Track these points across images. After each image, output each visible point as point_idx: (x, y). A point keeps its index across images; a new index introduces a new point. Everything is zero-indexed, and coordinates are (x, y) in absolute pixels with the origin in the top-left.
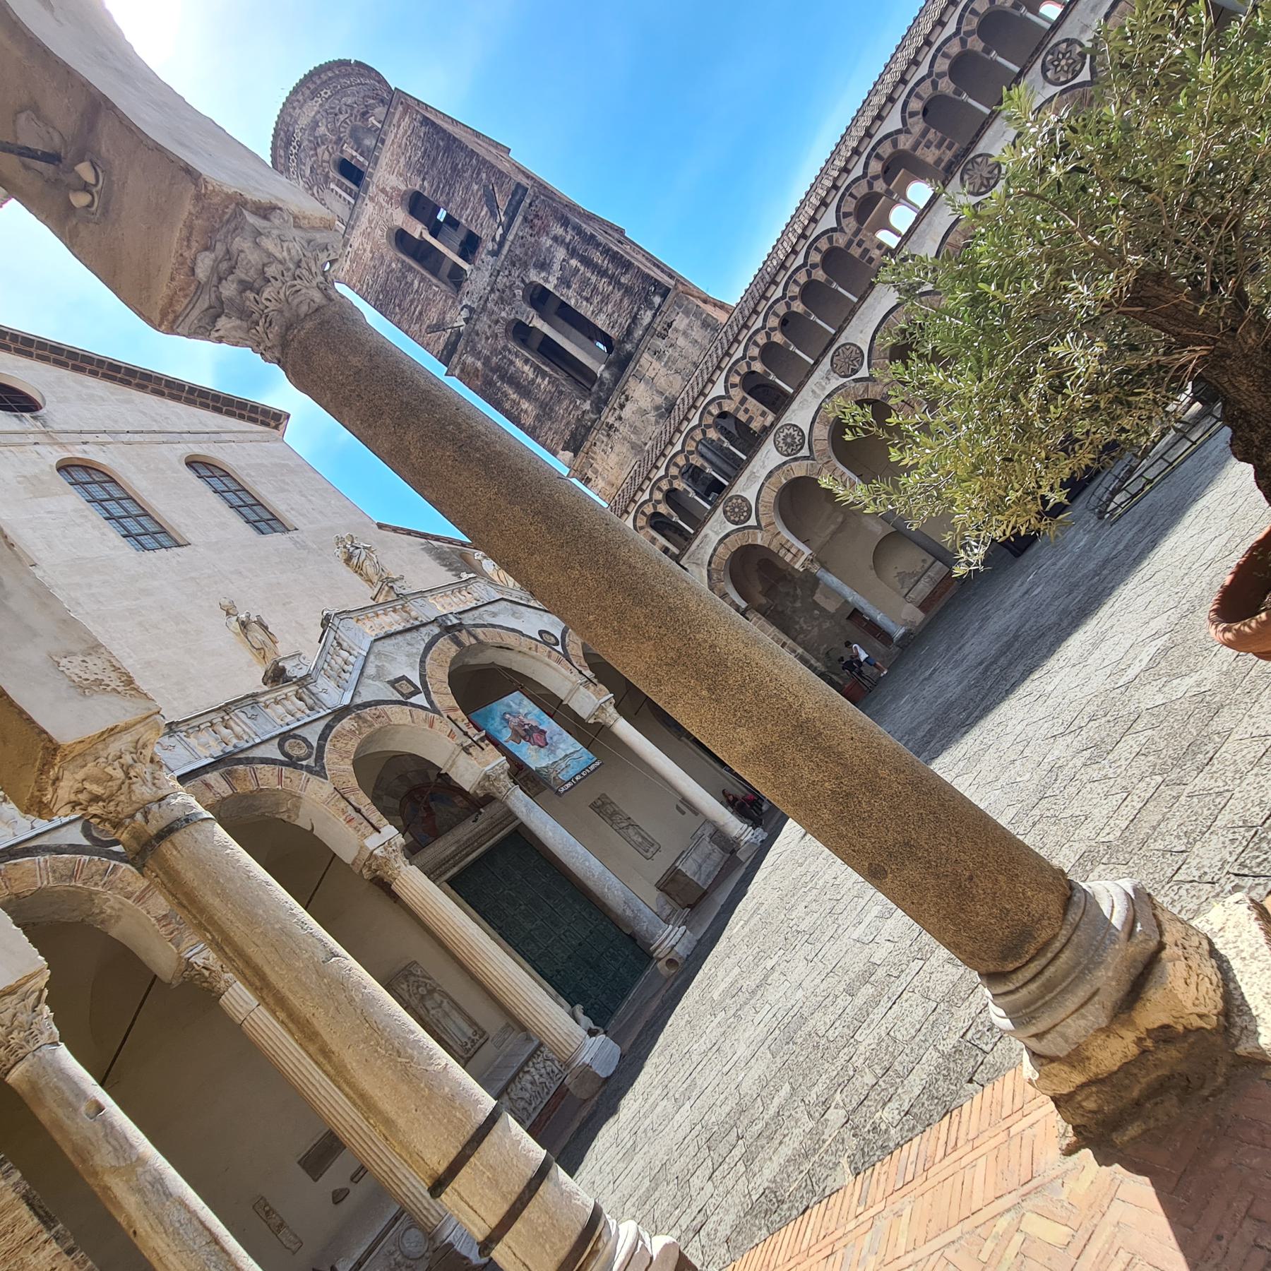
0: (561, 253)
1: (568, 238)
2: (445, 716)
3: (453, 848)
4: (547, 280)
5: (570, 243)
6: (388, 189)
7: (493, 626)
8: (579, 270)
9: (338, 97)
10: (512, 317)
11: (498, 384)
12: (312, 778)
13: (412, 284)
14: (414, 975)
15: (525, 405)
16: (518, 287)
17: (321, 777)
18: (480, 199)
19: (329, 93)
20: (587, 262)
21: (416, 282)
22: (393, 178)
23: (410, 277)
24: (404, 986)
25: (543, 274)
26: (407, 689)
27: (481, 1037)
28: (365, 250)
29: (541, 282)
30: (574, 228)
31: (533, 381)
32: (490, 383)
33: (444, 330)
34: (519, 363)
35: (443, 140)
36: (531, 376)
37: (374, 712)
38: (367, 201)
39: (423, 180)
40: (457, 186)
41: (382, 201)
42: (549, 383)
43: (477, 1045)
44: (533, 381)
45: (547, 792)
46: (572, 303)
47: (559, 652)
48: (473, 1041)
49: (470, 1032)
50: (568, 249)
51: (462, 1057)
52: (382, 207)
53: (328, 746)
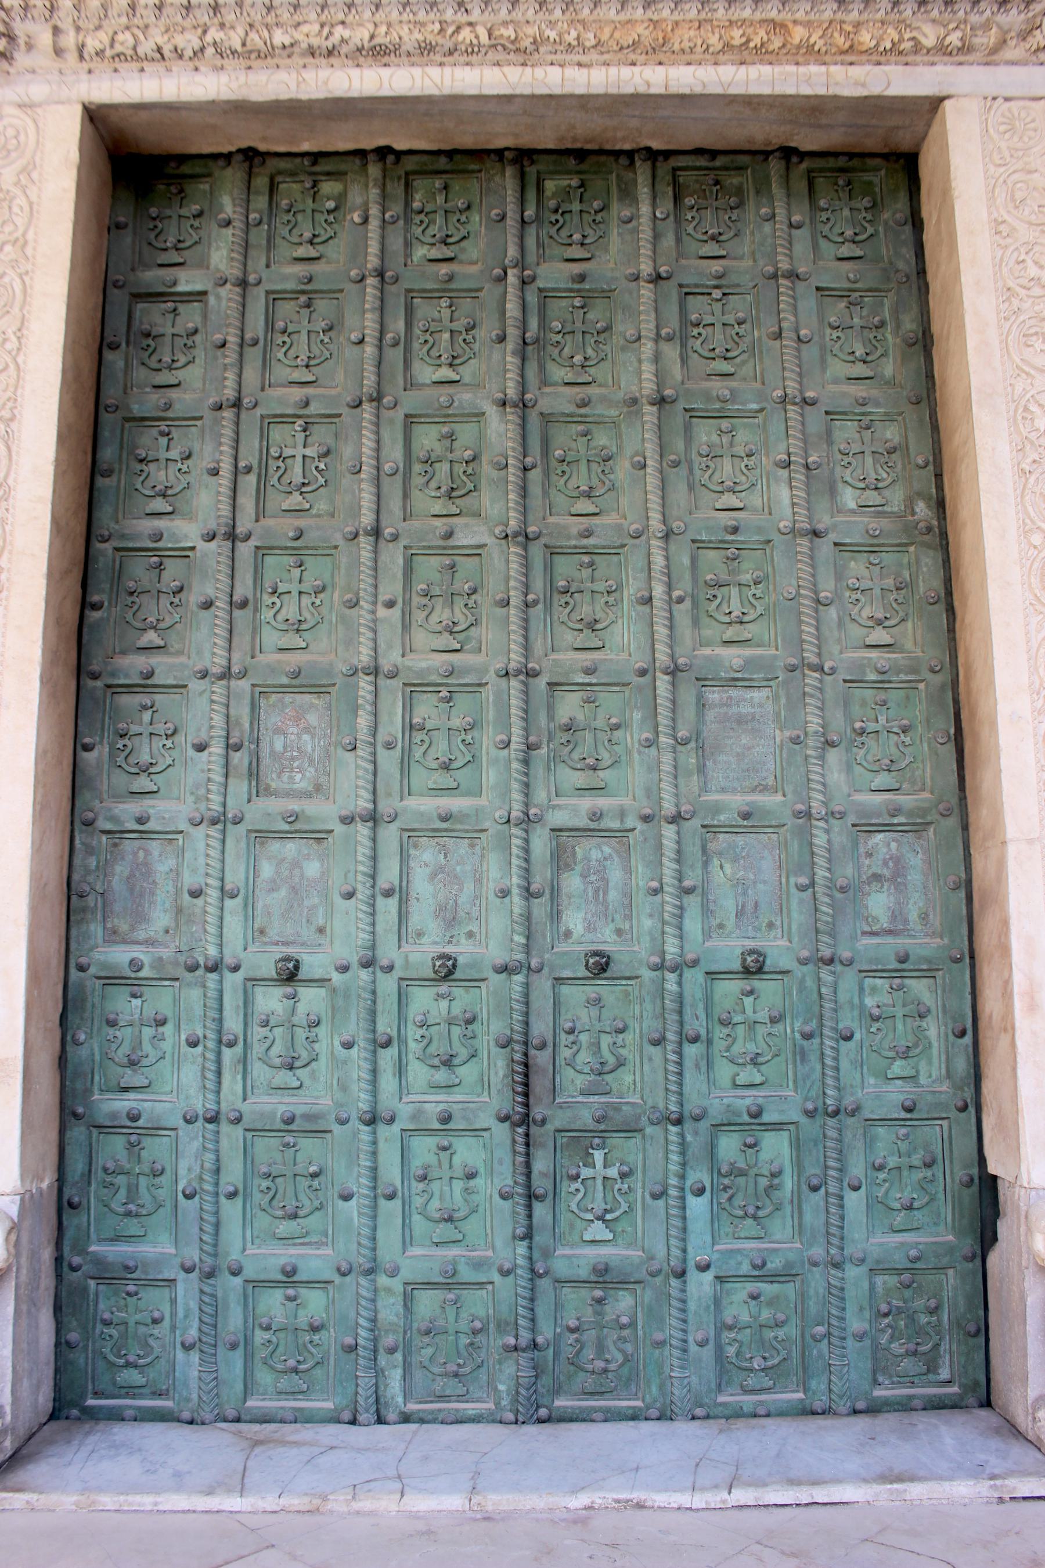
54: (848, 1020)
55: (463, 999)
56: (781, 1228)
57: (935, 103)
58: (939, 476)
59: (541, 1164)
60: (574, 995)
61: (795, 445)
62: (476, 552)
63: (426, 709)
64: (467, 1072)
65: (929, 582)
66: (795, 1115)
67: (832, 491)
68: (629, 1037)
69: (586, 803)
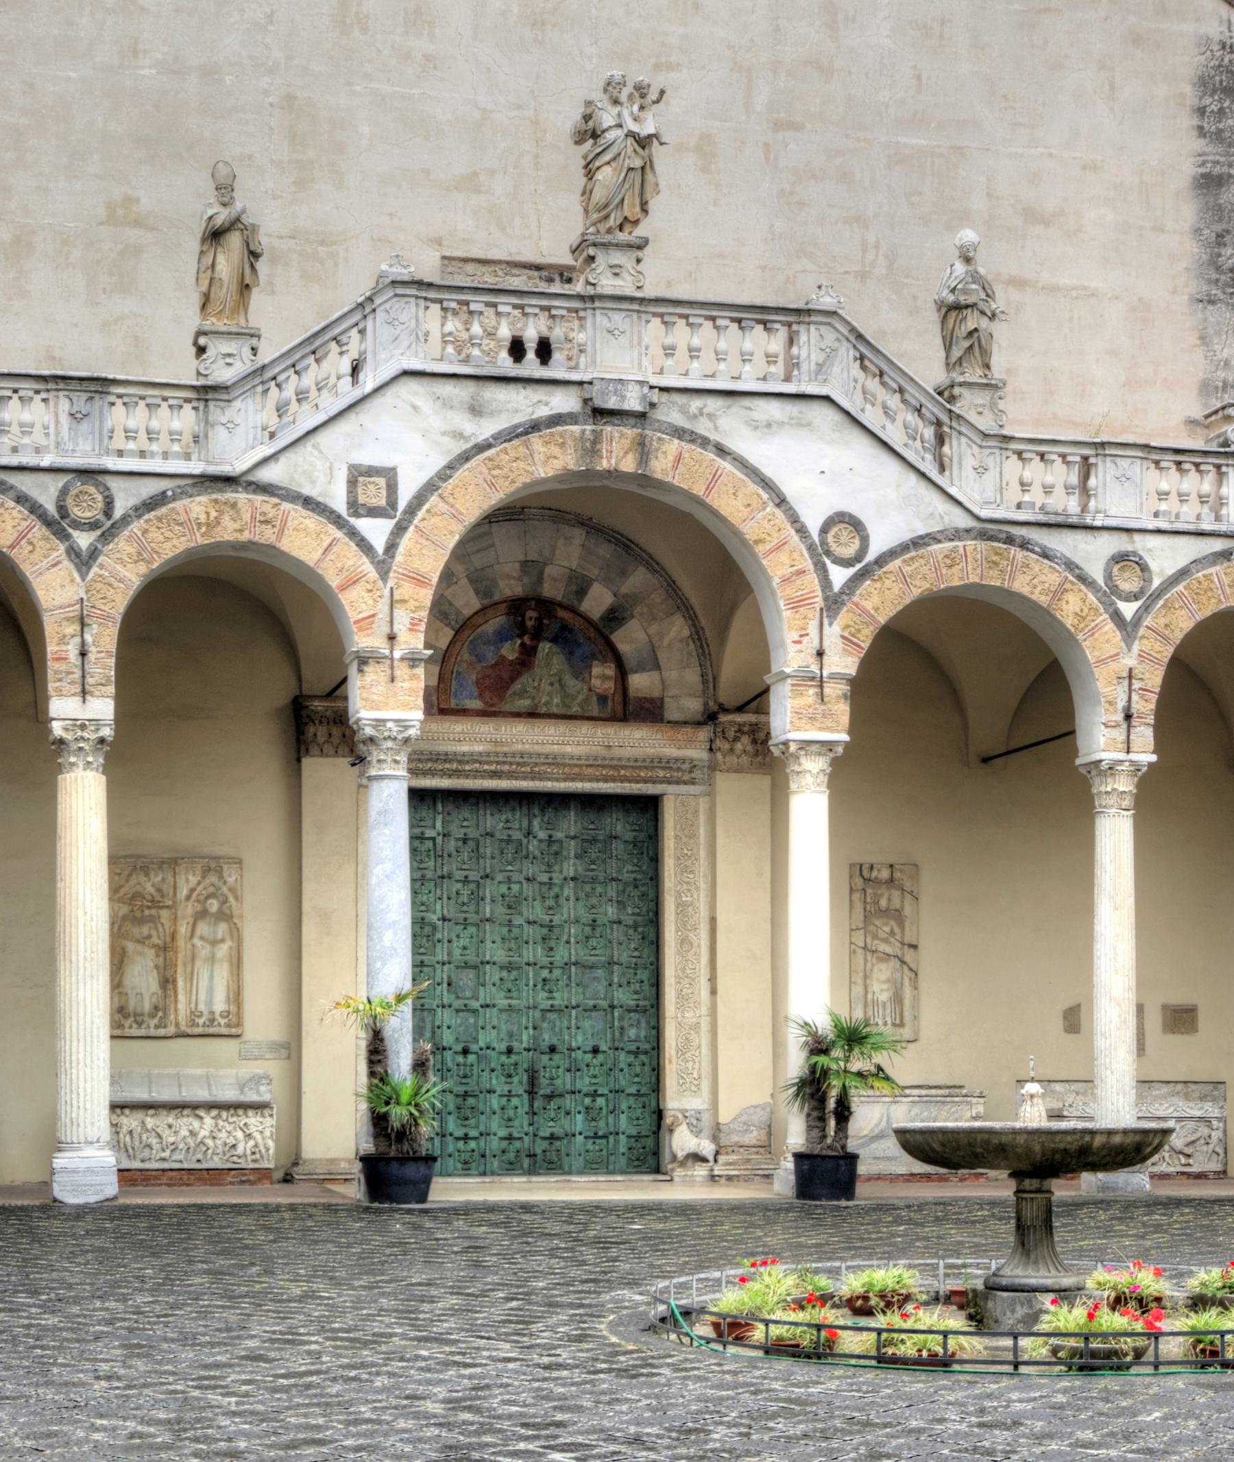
2: (391, 583)
3: (479, 748)
7: (721, 451)
12: (66, 564)
14: (221, 877)
17: (79, 570)
24: (193, 880)
26: (373, 494)
27: (228, 1026)
37: (267, 508)
43: (211, 1030)
45: (764, 782)
47: (826, 582)
48: (212, 1020)
49: (220, 1005)
51: (177, 1025)
53: (136, 527)
54: (622, 1065)
55: (514, 1058)
56: (602, 1124)
57: (662, 795)
58: (657, 904)
59: (536, 1105)
60: (545, 1058)
61: (614, 895)
62: (520, 926)
63: (504, 974)
64: (516, 1079)
65: (652, 936)
66: (606, 1092)
67: (625, 908)
68: (561, 1070)
69: (550, 1002)
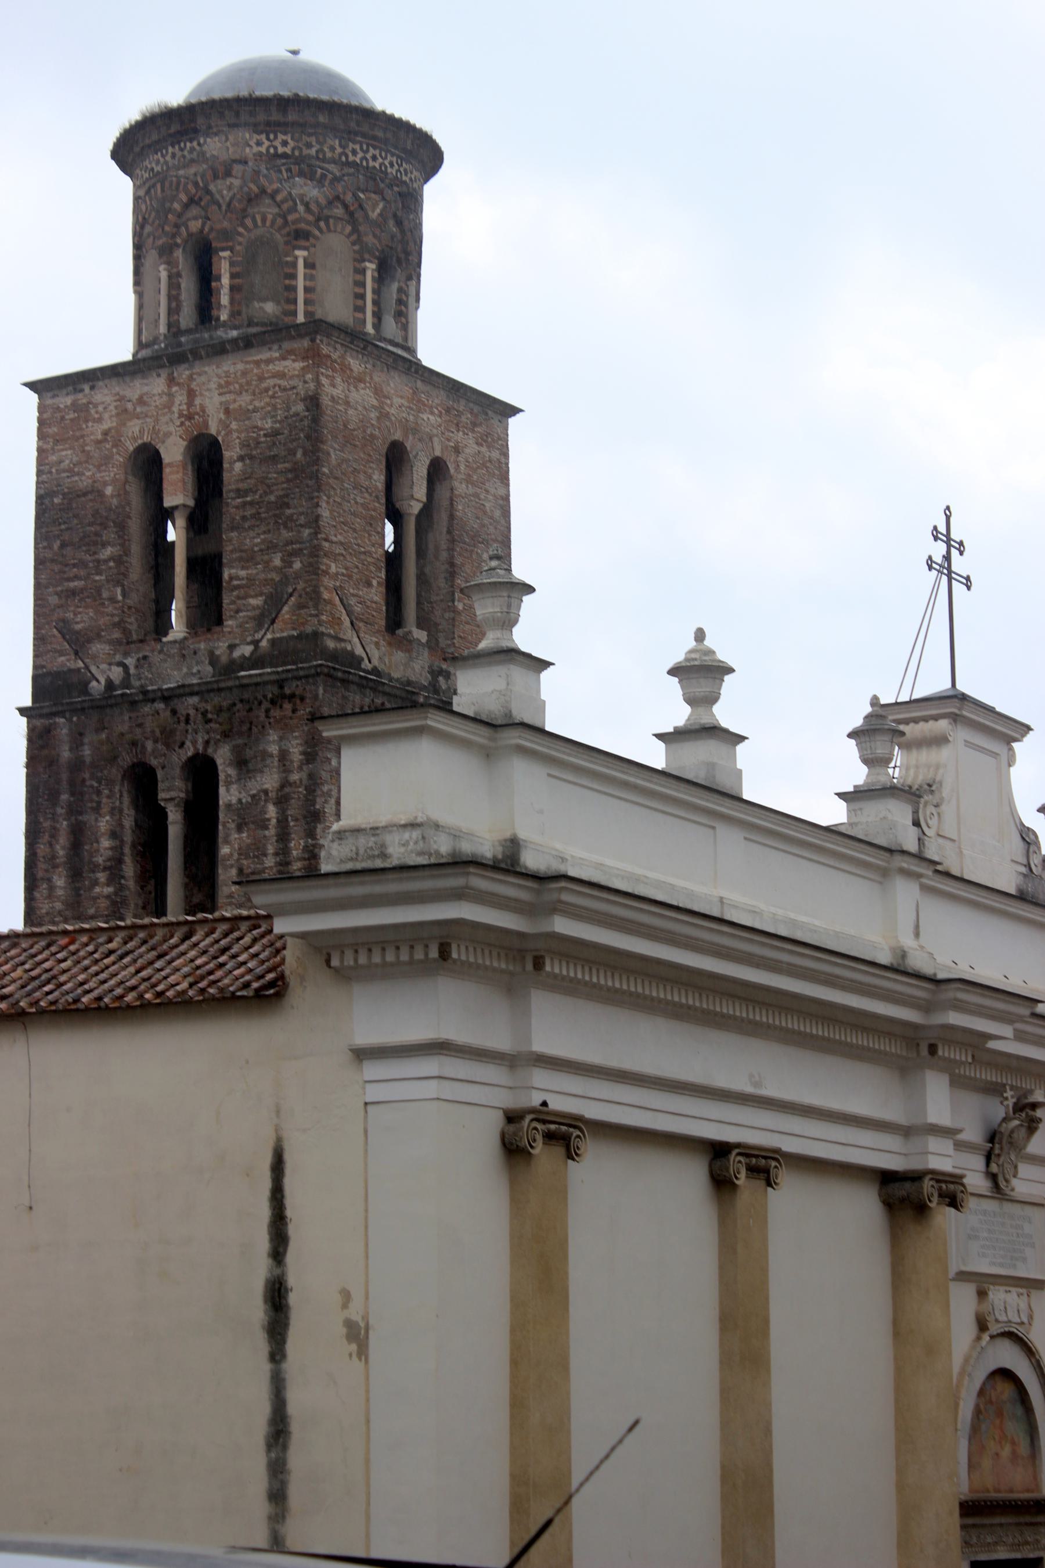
0: (269, 780)
1: (295, 777)
4: (228, 784)
5: (290, 785)
6: (198, 401)
8: (266, 828)
9: (295, 169)
10: (154, 762)
11: (60, 811)
13: (104, 545)
15: (60, 881)
16: (194, 743)
18: (267, 582)
19: (288, 150)
20: (283, 837)
21: (108, 552)
22: (217, 399)
23: (110, 535)
25: (232, 771)
28: (100, 420)
29: (222, 776)
30: (311, 776)
31: (95, 868)
32: (53, 797)
33: (76, 653)
34: (104, 823)
35: (305, 454)
36: (100, 860)
38: (164, 373)
39: (241, 458)
40: (263, 528)
41: (177, 402)
42: (108, 897)
44: (95, 868)
46: (224, 850)
50: (282, 787)
52: (169, 406)
